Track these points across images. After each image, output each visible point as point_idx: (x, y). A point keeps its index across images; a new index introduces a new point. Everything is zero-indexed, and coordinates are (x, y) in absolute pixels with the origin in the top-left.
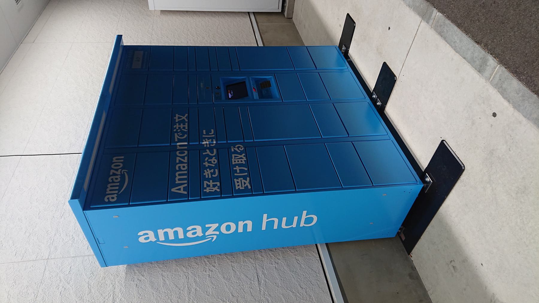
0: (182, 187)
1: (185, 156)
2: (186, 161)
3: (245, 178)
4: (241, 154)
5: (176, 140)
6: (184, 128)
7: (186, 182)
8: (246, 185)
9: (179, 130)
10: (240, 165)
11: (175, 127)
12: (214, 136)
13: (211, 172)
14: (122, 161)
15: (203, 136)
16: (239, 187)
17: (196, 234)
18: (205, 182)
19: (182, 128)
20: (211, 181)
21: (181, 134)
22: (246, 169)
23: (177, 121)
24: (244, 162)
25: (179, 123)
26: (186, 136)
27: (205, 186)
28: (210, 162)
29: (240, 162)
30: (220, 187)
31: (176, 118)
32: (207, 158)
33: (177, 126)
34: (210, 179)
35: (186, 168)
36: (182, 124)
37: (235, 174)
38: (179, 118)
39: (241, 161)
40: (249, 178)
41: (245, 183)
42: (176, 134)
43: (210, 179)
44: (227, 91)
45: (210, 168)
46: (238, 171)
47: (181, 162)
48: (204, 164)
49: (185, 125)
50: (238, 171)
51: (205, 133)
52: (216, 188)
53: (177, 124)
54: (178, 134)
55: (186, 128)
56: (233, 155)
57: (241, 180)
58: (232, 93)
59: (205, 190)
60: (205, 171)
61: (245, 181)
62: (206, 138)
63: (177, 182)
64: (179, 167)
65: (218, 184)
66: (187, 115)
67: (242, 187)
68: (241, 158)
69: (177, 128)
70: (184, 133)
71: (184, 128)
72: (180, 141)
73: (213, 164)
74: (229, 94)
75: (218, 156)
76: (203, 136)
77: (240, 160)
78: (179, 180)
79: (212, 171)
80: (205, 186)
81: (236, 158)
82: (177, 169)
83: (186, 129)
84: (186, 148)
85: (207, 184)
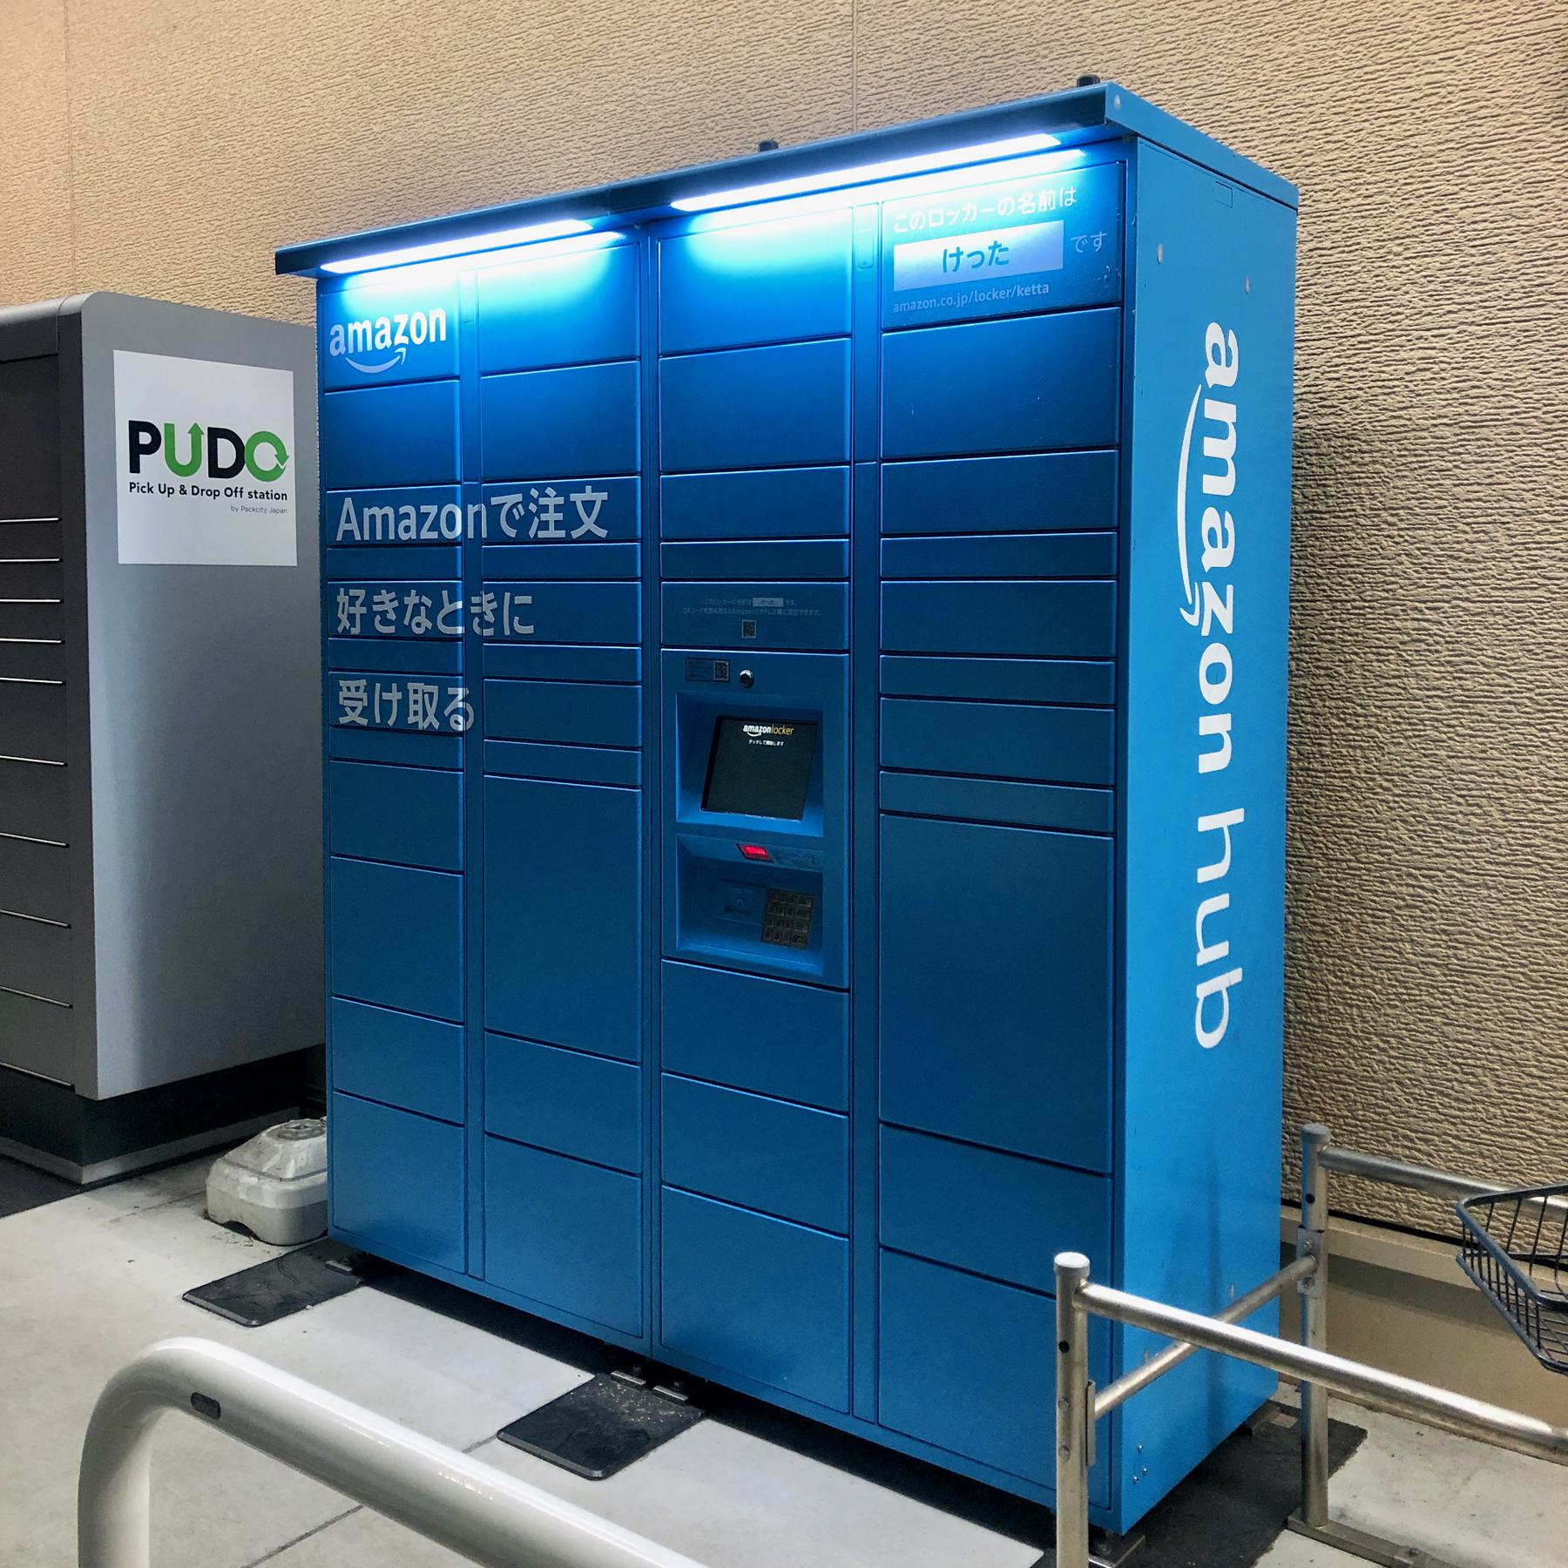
0: (354, 526)
1: (440, 534)
2: (426, 535)
3: (367, 712)
4: (439, 714)
5: (495, 501)
6: (544, 525)
7: (367, 537)
8: (347, 709)
9: (533, 507)
10: (404, 703)
11: (549, 491)
12: (507, 632)
13: (387, 611)
14: (432, 339)
15: (507, 595)
16: (345, 689)
17: (1212, 546)
18: (361, 593)
19: (544, 517)
20: (364, 610)
21: (517, 517)
22: (391, 722)
23: (573, 497)
24: (411, 719)
25: (568, 508)
26: (512, 533)
27: (352, 592)
28: (416, 612)
29: (412, 707)
30: (346, 634)
31: (588, 494)
32: (428, 602)
33: (552, 499)
34: (370, 609)
35: (404, 537)
36: (560, 516)
37: (378, 686)
38: (588, 506)
39: (416, 713)
40: (366, 724)
41: (353, 709)
42: (518, 497)
43: (370, 609)
44: (788, 724)
45: (399, 612)
46: (386, 696)
47: (422, 518)
48: (413, 592)
49: (556, 528)
50: (386, 696)
51: (519, 600)
52: (345, 623)
53: (561, 500)
54: (520, 506)
55: (542, 534)
56: (434, 689)
57: (361, 700)
58: (769, 743)
59: (342, 590)
60: (393, 595)
61: (358, 711)
62: (501, 605)
63: (367, 512)
64: (407, 516)
65: (356, 631)
66: (602, 533)
67: (345, 698)
68: (425, 715)
69: (542, 501)
70: (523, 524)
71: (544, 525)
72: (494, 511)
73: (411, 621)
74: (768, 730)
75: (433, 637)
76: (507, 595)
77: (419, 707)
78: (373, 517)
79: (392, 616)
80: (352, 592)
81: (426, 696)
82: (402, 510)
83: (536, 533)
84: (471, 535)
85: (358, 597)
